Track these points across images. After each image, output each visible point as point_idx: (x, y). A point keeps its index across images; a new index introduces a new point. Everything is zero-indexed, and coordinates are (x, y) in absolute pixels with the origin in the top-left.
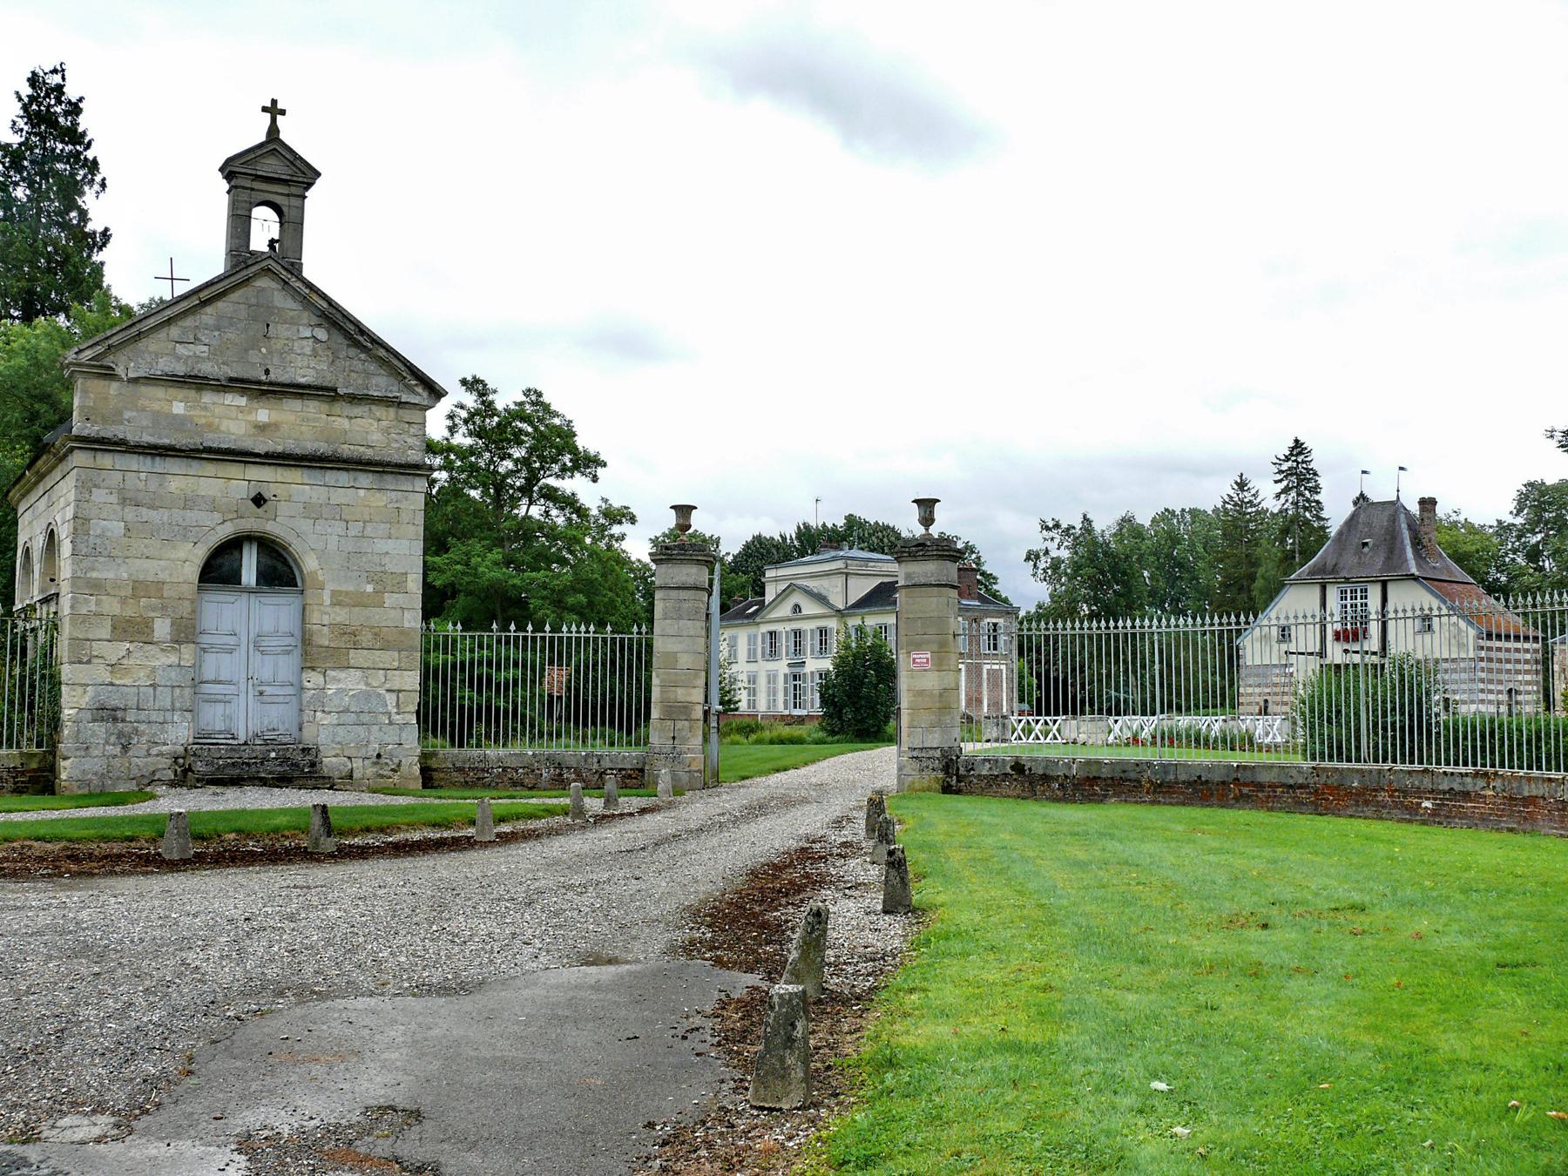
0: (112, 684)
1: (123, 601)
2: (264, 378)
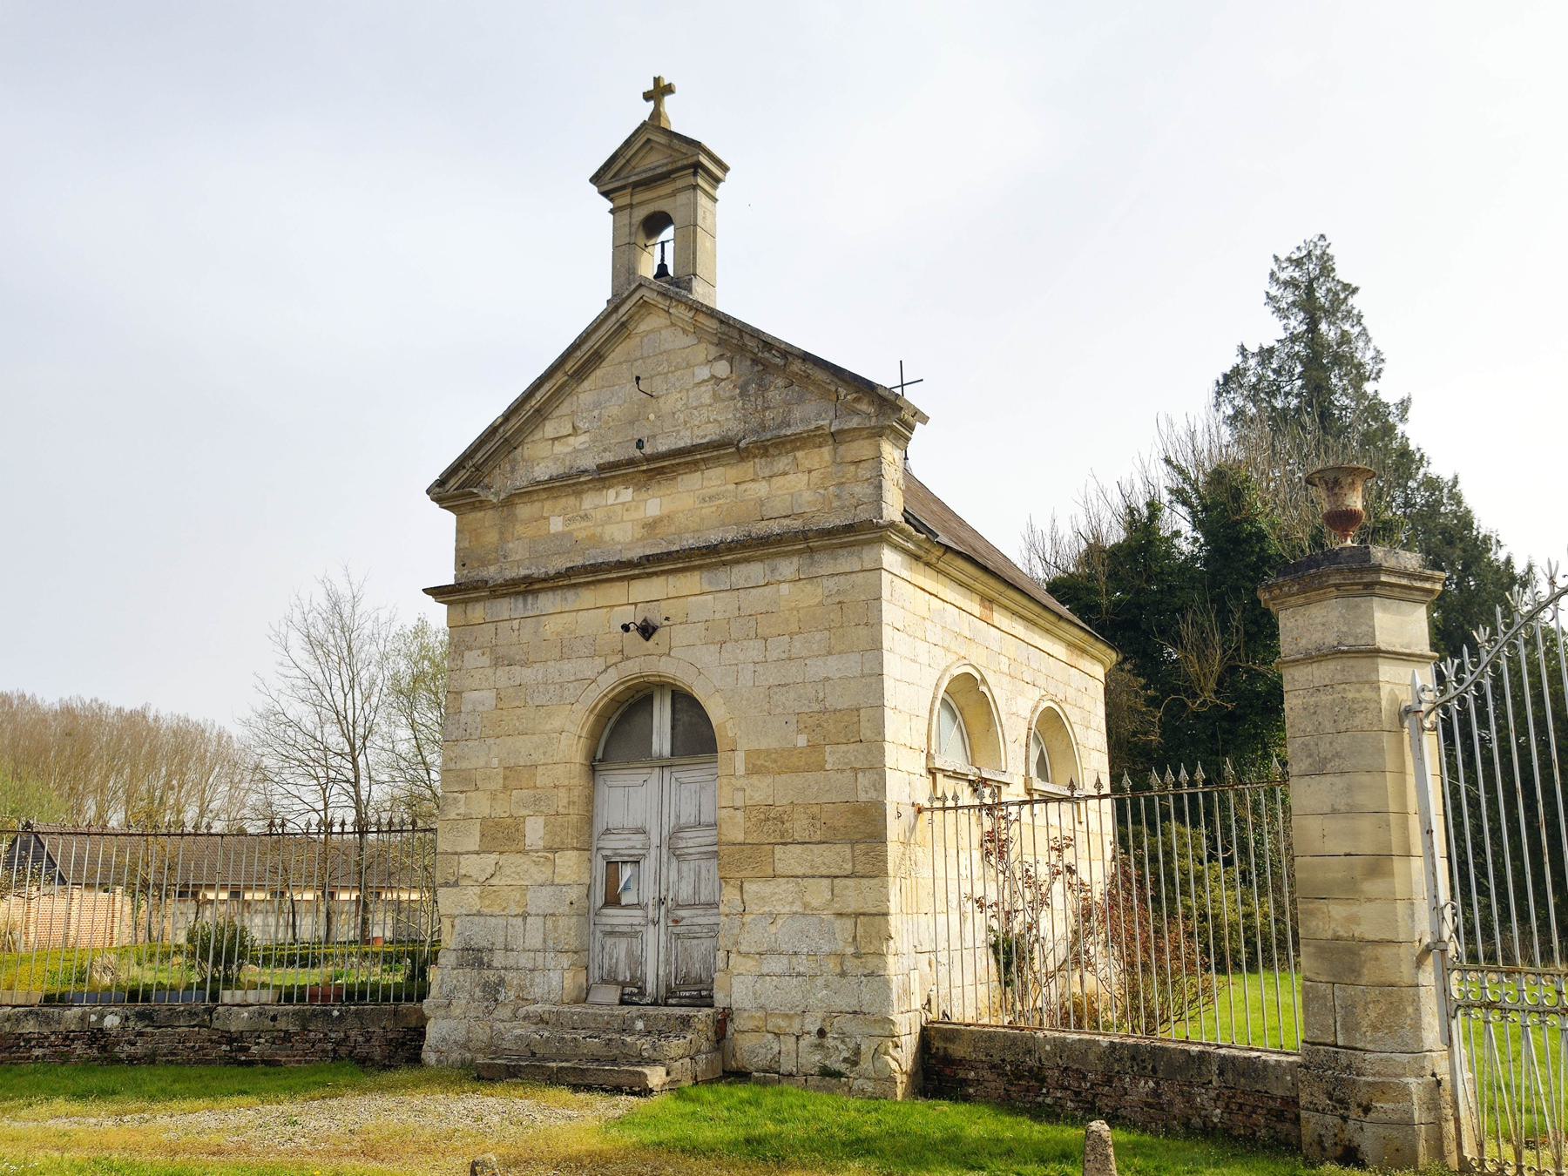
0: (479, 914)
1: (493, 796)
2: (638, 453)
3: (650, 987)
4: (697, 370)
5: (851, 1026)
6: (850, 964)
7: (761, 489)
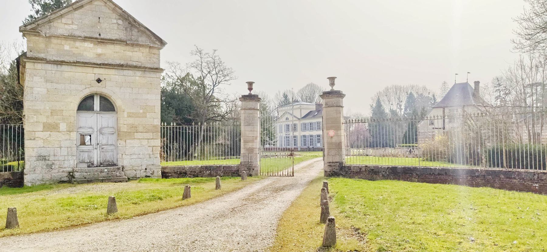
0: (43, 147)
1: (48, 117)
2: (98, 36)
3: (95, 163)
4: (113, 20)
5: (152, 167)
6: (152, 156)
7: (129, 54)
